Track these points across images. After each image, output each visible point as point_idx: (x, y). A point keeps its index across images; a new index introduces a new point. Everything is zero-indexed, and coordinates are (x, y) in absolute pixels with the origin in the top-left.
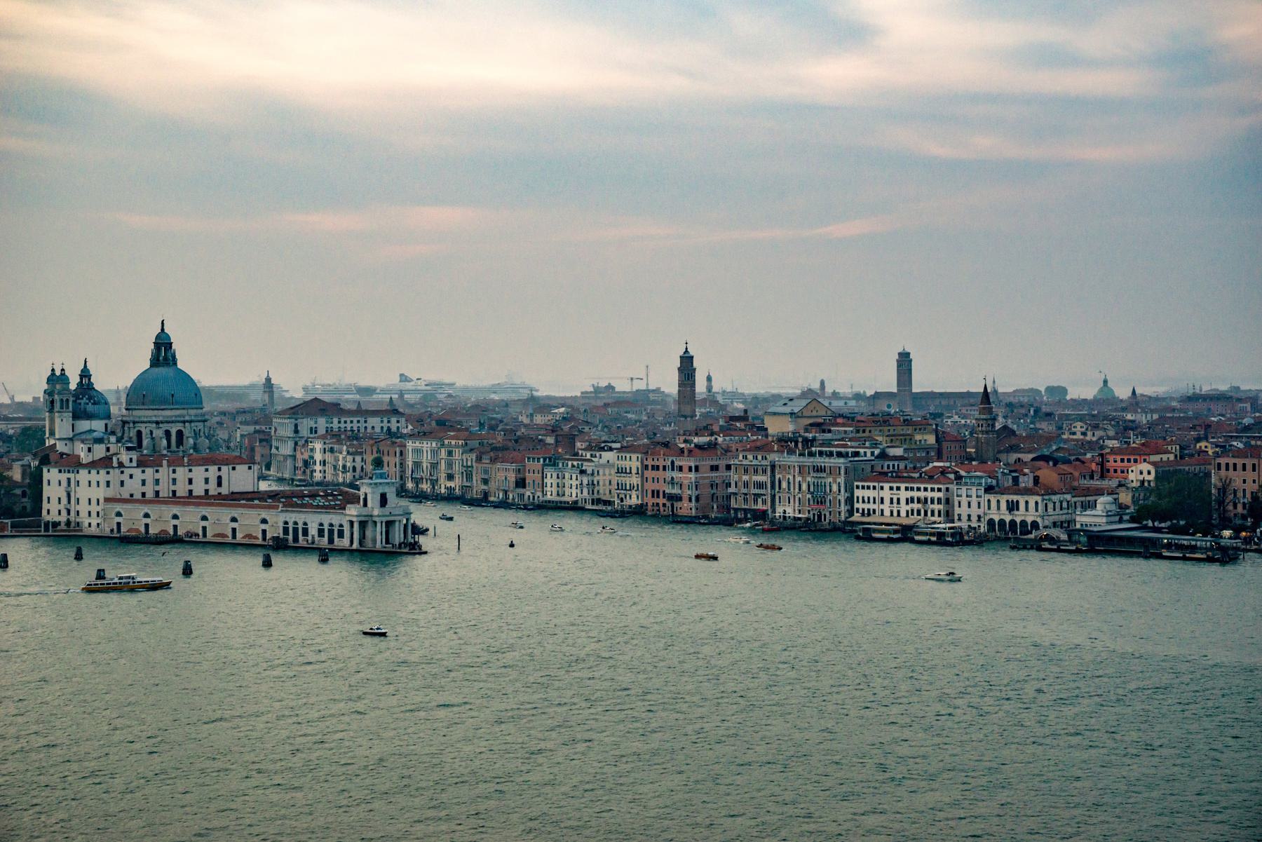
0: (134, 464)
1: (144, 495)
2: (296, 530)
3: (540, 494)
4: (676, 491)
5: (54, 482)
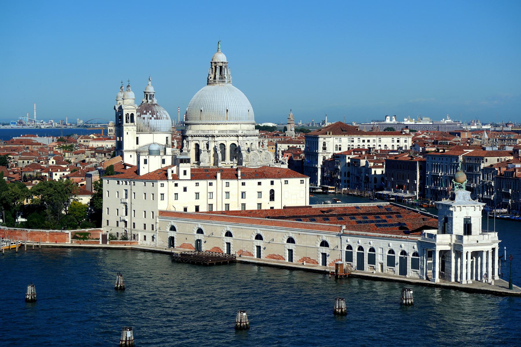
0: (188, 176)
1: (197, 208)
2: (361, 256)
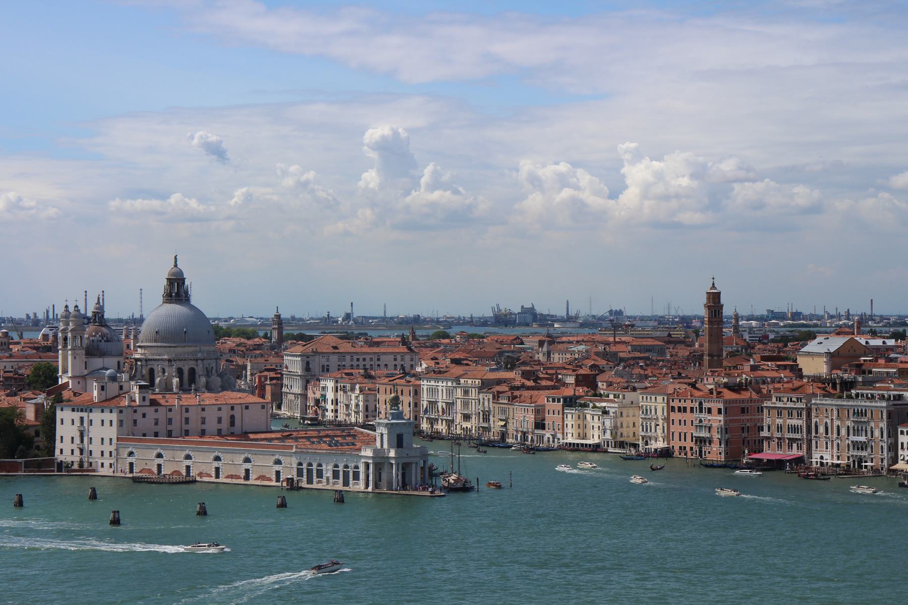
2: (310, 472)
3: (559, 436)
4: (704, 434)
5: (67, 422)
